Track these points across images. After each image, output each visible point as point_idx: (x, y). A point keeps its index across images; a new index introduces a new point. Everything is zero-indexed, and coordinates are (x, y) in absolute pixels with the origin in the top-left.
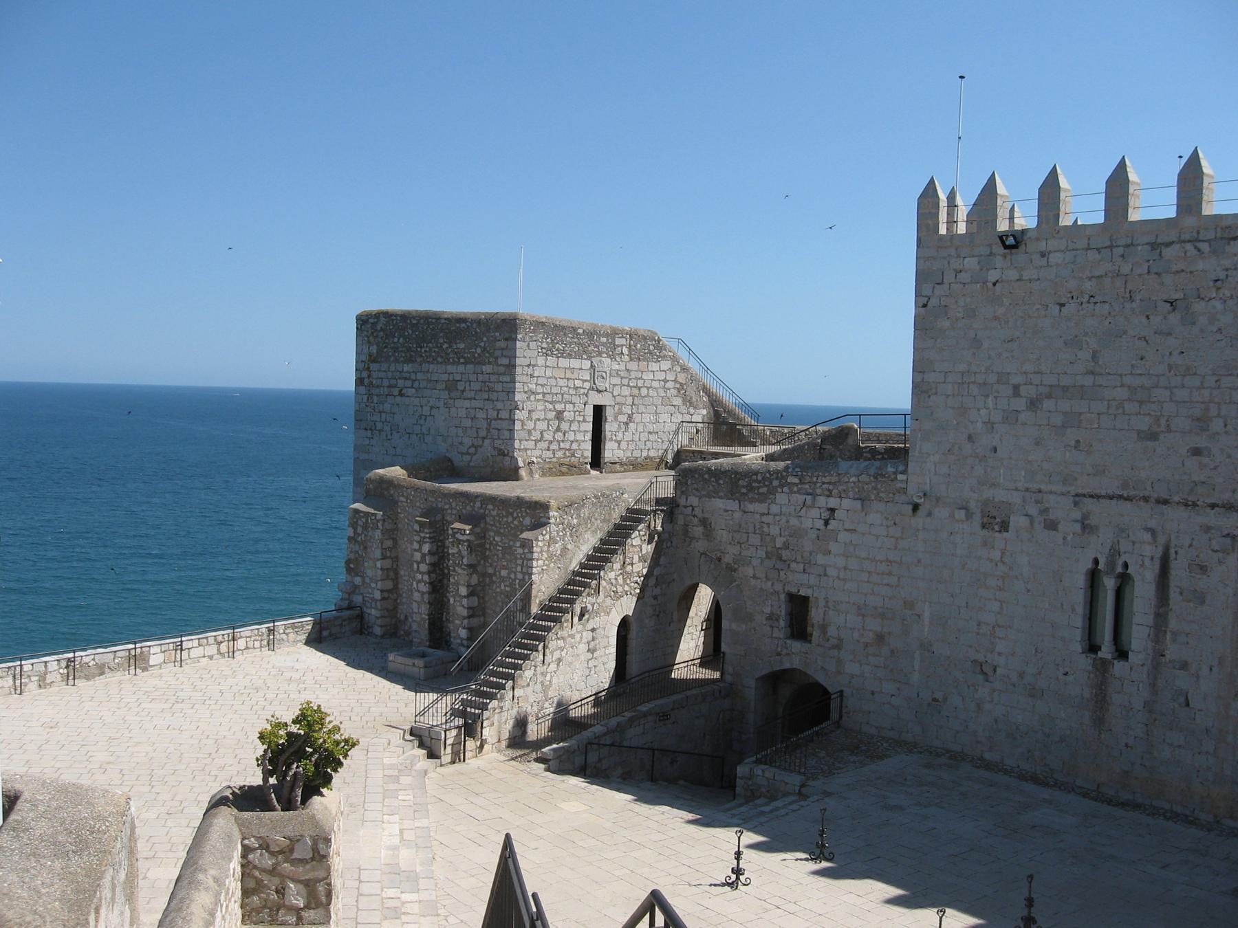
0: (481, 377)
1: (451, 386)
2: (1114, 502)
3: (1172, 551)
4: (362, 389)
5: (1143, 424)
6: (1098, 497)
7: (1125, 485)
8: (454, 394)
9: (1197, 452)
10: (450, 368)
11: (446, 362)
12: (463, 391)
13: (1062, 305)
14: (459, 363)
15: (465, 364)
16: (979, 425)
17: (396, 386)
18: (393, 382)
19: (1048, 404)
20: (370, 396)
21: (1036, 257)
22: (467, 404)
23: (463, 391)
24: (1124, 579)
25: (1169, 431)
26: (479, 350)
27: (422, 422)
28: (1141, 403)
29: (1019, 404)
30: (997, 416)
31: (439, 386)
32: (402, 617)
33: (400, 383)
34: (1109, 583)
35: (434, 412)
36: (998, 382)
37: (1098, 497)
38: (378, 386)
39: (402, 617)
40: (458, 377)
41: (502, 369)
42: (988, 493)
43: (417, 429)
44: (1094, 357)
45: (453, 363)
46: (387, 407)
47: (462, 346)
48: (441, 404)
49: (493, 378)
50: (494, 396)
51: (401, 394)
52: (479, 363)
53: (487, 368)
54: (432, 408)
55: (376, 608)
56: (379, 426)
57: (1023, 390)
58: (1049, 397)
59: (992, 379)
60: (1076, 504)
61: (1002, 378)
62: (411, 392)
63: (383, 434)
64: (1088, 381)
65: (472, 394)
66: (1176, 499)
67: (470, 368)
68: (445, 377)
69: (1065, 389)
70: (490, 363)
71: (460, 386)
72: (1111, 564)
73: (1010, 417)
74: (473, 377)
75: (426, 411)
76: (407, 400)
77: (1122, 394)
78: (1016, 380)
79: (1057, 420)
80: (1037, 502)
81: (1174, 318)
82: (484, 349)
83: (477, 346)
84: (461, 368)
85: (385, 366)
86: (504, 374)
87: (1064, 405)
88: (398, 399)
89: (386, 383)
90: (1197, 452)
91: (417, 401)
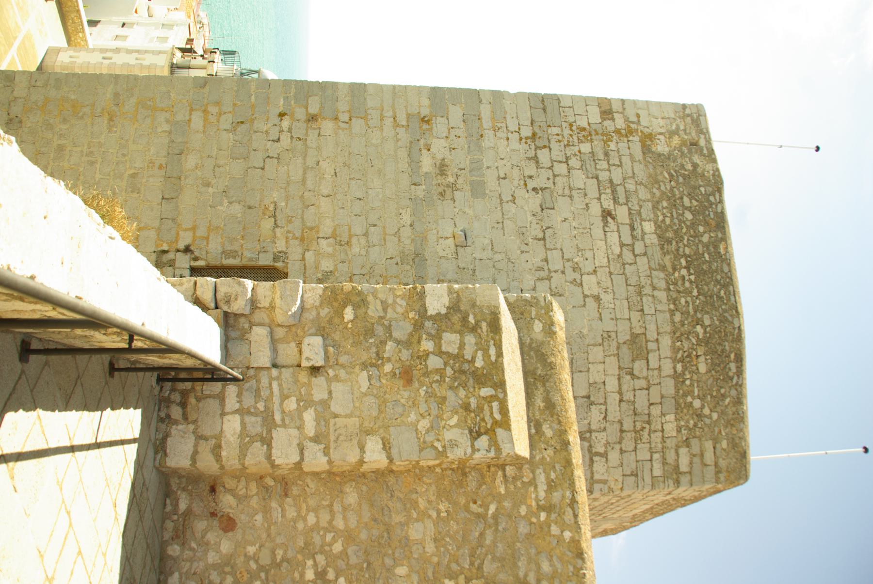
0: (656, 411)
1: (638, 346)
4: (595, 116)
8: (625, 351)
10: (666, 341)
11: (677, 335)
12: (631, 374)
14: (675, 360)
15: (676, 376)
17: (615, 200)
18: (620, 190)
20: (586, 134)
22: (612, 384)
23: (631, 374)
26: (697, 404)
27: (571, 275)
31: (635, 316)
32: (227, 502)
33: (622, 213)
35: (591, 303)
38: (606, 154)
39: (227, 502)
40: (654, 363)
41: (671, 457)
43: (556, 263)
45: (676, 350)
46: (579, 179)
47: (703, 368)
48: (609, 326)
49: (657, 437)
50: (628, 444)
51: (607, 214)
52: (678, 404)
53: (670, 428)
54: (597, 298)
55: (246, 439)
56: (544, 156)
62: (613, 238)
63: (531, 170)
65: (628, 396)
67: (669, 388)
68: (652, 335)
70: (679, 430)
71: (639, 366)
74: (655, 392)
75: (590, 284)
76: (598, 232)
82: (700, 416)
83: (702, 398)
84: (667, 367)
85: (641, 172)
86: (664, 463)
88: (596, 210)
89: (617, 175)
91: (601, 260)
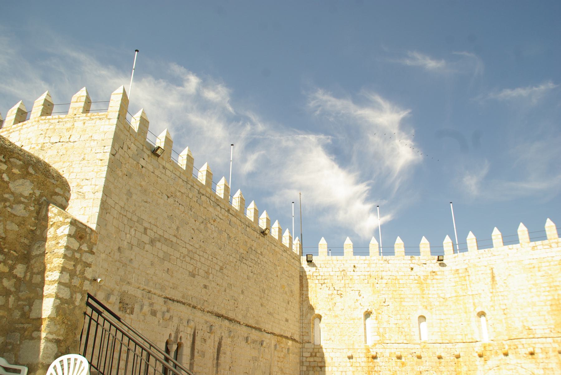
2: (179, 304)
3: (196, 331)
5: (191, 268)
6: (173, 300)
7: (183, 297)
9: (205, 287)
13: (168, 197)
16: (125, 243)
19: (158, 245)
21: (161, 167)
24: (179, 346)
25: (198, 275)
28: (191, 258)
29: (146, 239)
30: (135, 242)
34: (175, 347)
36: (138, 222)
37: (173, 300)
42: (125, 288)
44: (178, 228)
57: (149, 231)
58: (159, 241)
59: (135, 218)
60: (165, 302)
61: (140, 221)
64: (174, 240)
66: (199, 307)
69: (166, 240)
72: (176, 337)
73: (141, 245)
77: (185, 251)
78: (146, 225)
79: (161, 255)
80: (149, 298)
81: (202, 226)
87: (165, 248)
90: (205, 287)
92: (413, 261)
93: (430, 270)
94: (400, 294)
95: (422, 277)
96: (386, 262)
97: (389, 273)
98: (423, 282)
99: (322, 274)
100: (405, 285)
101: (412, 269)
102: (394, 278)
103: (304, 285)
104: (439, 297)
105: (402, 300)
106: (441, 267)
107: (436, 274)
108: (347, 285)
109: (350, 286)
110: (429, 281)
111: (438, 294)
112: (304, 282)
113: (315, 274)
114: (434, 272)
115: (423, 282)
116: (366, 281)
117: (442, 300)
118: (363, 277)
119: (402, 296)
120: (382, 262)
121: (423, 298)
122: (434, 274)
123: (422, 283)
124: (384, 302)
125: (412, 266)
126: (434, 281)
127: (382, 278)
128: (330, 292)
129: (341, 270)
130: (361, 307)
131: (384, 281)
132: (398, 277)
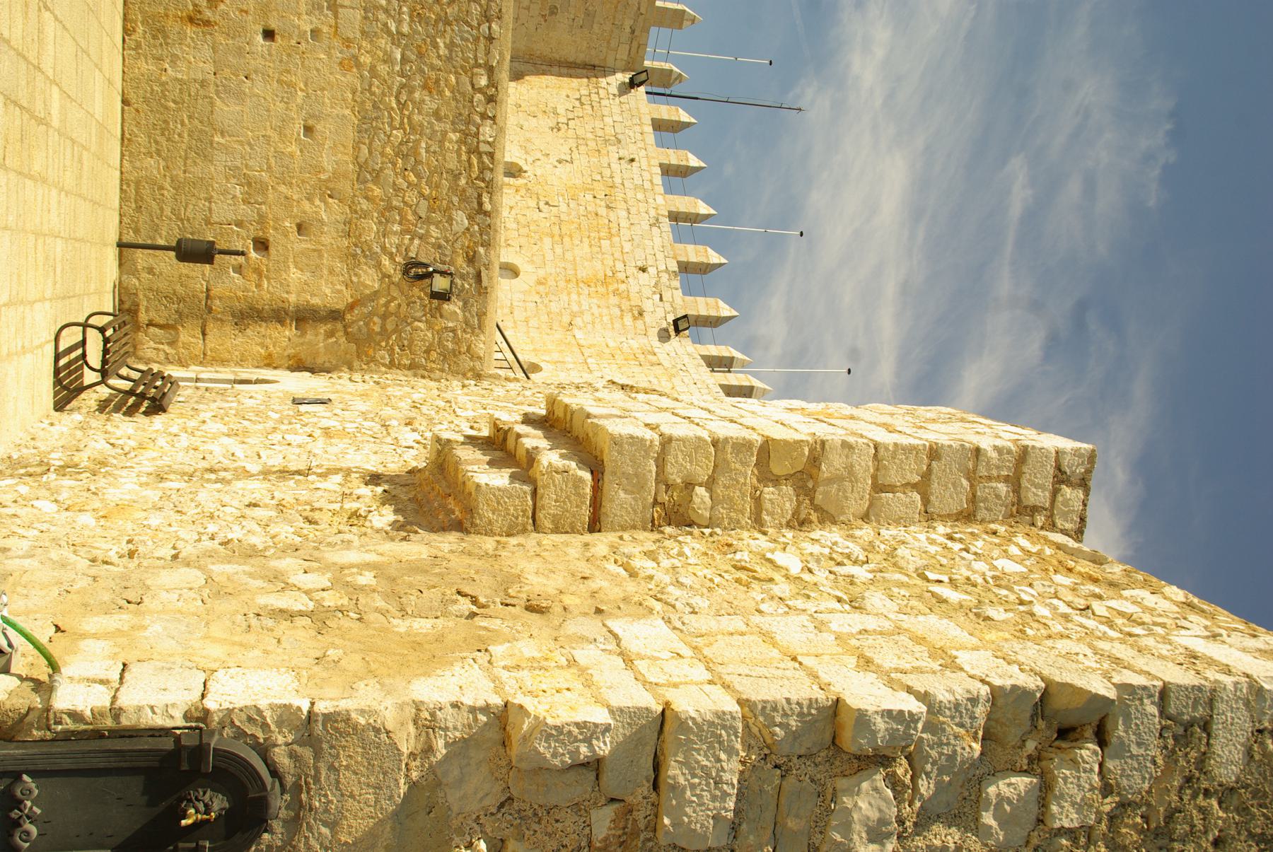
92: (665, 277)
93: (647, 306)
94: (571, 236)
95: (622, 287)
96: (652, 221)
97: (624, 224)
98: (611, 288)
99: (604, 102)
100: (596, 249)
101: (643, 270)
102: (614, 231)
103: (572, 71)
104: (574, 315)
105: (557, 238)
106: (656, 330)
107: (635, 319)
108: (580, 142)
109: (582, 148)
110: (614, 300)
111: (582, 312)
112: (579, 71)
113: (601, 91)
114: (641, 314)
115: (611, 288)
116: (599, 177)
117: (566, 319)
118: (607, 173)
119: (567, 239)
120: (653, 213)
121: (568, 281)
122: (636, 313)
123: (605, 283)
124: (547, 203)
125: (652, 270)
126: (617, 311)
127: (608, 207)
128: (561, 110)
129: (620, 137)
130: (530, 160)
131: (602, 211)
132: (616, 239)
